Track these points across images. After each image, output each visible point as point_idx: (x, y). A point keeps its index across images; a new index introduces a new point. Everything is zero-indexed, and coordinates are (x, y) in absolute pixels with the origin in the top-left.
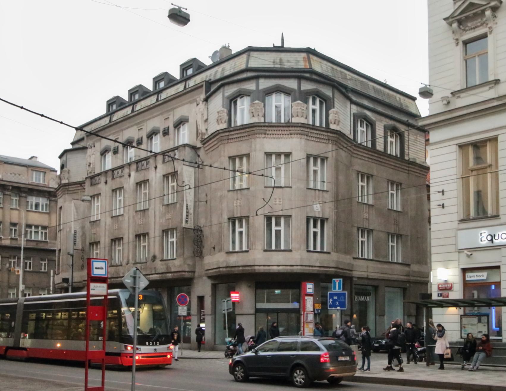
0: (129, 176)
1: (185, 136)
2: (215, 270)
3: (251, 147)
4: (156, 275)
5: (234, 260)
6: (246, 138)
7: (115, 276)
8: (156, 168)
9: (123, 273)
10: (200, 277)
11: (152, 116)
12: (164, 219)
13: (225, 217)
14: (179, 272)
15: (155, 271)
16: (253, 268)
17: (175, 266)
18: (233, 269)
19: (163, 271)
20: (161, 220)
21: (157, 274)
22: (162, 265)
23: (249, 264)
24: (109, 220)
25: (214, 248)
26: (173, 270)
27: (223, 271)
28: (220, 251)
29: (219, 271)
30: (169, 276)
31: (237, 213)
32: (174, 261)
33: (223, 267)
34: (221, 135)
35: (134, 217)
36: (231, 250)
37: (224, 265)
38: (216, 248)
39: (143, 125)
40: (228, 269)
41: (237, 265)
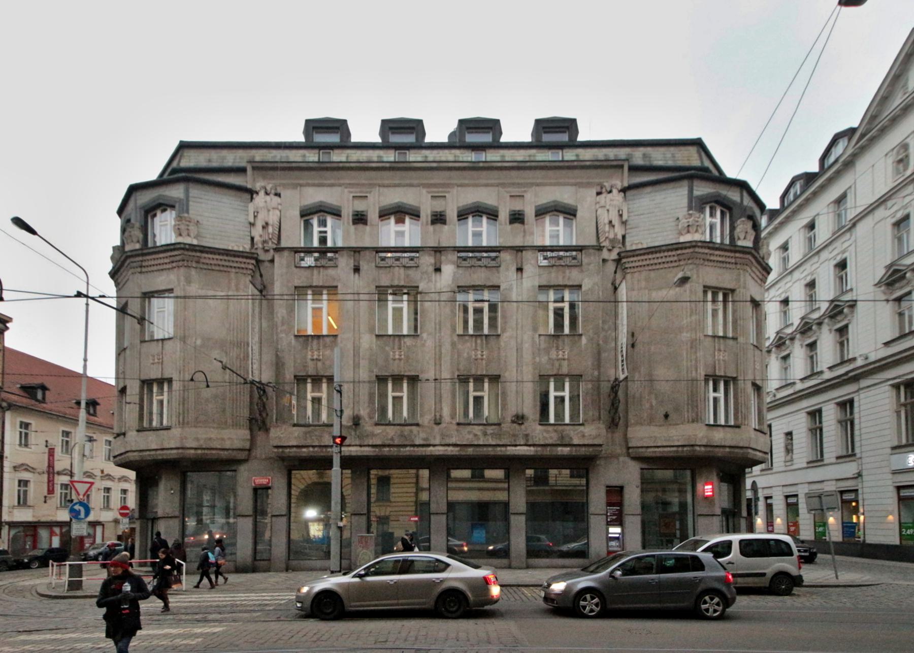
0: (438, 270)
1: (553, 232)
2: (674, 449)
3: (738, 280)
4: (526, 448)
5: (719, 437)
6: (731, 266)
7: (396, 442)
8: (520, 270)
9: (424, 439)
10: (613, 456)
11: (472, 182)
12: (544, 359)
13: (702, 372)
14: (584, 445)
15: (527, 440)
16: (745, 450)
17: (583, 436)
18: (717, 450)
19: (550, 441)
20: (537, 359)
21: (530, 446)
22: (548, 432)
23: (741, 445)
24: (367, 341)
25: (666, 416)
26: (576, 441)
27: (699, 451)
28: (695, 420)
29: (683, 451)
30: (566, 450)
31: (719, 370)
32: (582, 428)
33: (700, 446)
34: (697, 250)
35: (453, 344)
36: (712, 422)
37: (704, 442)
38: (673, 416)
39: (449, 192)
40: (709, 449)
41: (723, 444)
